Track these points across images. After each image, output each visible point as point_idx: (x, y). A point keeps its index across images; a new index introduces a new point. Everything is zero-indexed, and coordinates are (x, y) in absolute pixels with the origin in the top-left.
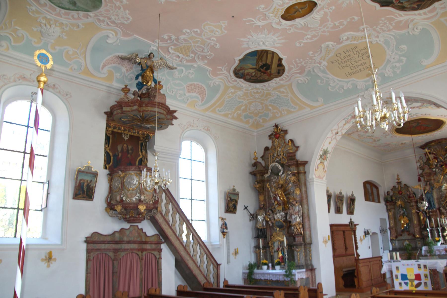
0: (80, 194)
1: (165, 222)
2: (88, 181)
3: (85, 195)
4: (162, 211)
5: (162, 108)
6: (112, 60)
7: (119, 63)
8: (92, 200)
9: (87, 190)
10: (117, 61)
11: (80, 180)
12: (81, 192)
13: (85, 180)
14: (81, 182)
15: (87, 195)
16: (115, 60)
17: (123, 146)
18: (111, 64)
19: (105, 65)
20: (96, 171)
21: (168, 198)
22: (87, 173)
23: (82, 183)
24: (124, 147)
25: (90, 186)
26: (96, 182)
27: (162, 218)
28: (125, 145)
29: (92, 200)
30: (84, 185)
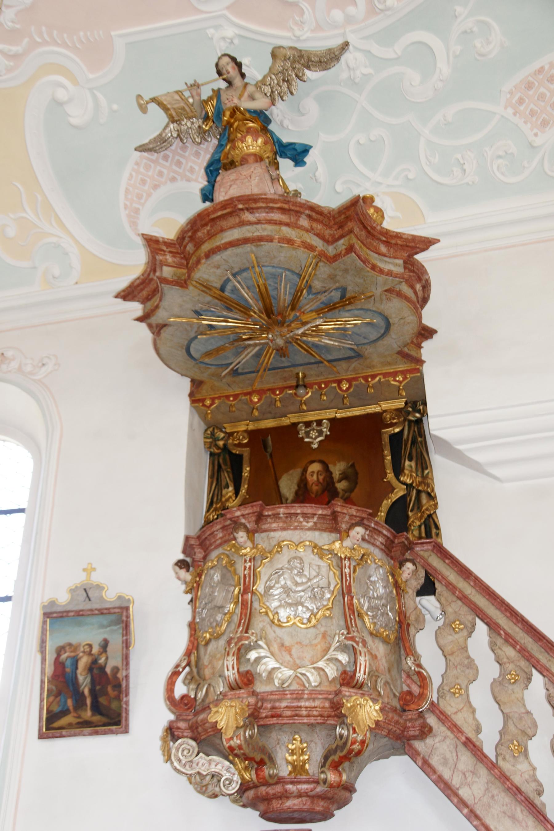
0: (65, 713)
1: (498, 792)
2: (90, 646)
3: (88, 714)
4: (478, 730)
5: (262, 215)
6: (143, 182)
7: (172, 174)
8: (126, 731)
9: (93, 692)
10: (161, 174)
11: (60, 650)
12: (70, 703)
13: (79, 645)
14: (64, 656)
15: (96, 708)
16: (150, 173)
17: (305, 470)
18: (149, 195)
19: (137, 211)
20: (120, 598)
21: (510, 652)
22: (79, 614)
23: (68, 663)
24: (309, 478)
25: (102, 669)
26: (127, 644)
27: (483, 772)
28: (315, 467)
29: (126, 731)
30: (77, 668)
